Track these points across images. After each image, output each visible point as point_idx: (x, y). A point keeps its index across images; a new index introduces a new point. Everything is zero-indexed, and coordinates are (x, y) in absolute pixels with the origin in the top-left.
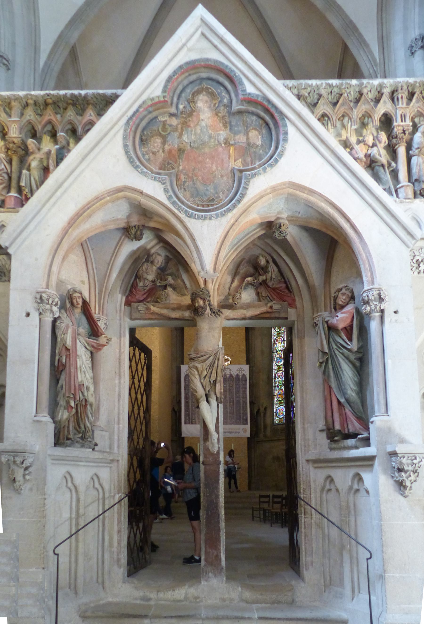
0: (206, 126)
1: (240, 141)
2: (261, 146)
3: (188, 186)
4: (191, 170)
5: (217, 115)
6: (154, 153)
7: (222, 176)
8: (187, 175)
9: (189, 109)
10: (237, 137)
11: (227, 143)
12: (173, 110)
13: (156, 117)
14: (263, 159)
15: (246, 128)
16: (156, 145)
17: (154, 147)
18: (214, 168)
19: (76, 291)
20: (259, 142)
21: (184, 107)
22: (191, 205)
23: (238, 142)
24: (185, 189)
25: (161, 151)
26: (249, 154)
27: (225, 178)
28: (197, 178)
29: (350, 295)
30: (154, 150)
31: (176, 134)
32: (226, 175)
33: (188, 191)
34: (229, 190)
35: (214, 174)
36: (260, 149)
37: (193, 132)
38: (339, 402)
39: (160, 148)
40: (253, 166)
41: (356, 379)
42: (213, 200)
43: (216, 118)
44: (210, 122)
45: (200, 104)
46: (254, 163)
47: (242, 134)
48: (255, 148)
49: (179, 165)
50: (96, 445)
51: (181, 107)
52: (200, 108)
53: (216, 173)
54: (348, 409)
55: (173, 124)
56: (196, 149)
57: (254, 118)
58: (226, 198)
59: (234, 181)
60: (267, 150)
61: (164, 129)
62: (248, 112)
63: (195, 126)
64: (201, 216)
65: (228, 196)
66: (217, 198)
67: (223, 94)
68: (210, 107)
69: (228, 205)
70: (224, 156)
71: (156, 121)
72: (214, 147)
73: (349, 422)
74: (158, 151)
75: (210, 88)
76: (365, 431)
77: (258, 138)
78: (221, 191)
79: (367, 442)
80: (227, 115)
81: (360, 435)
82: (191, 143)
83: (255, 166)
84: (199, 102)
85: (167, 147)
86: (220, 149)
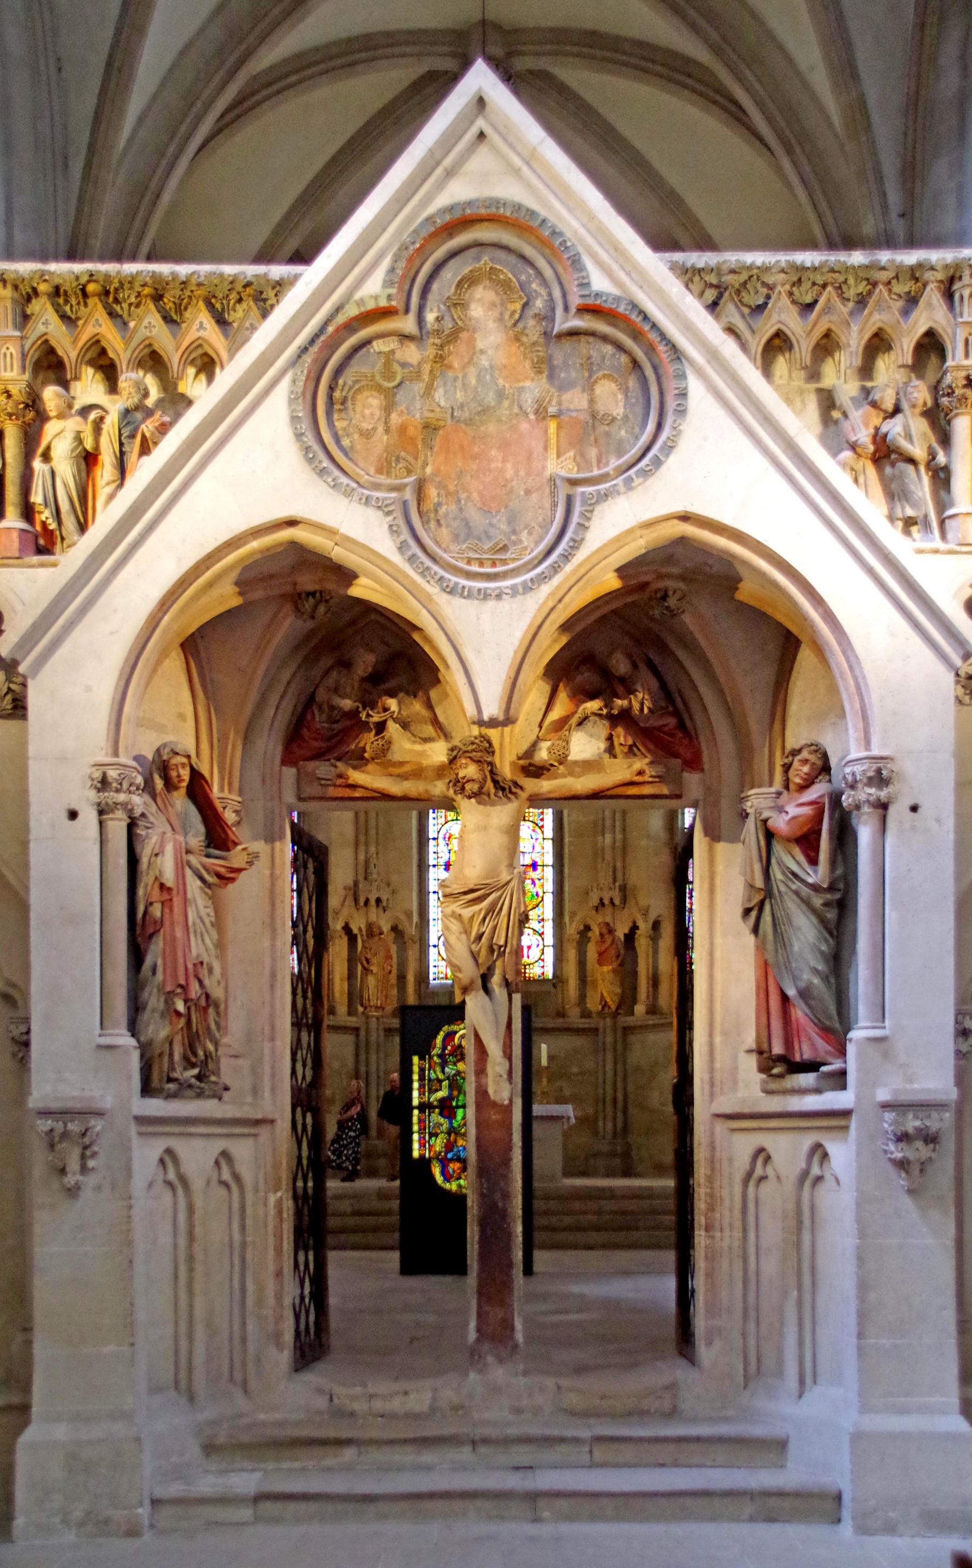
0: (492, 367)
1: (572, 407)
2: (622, 419)
3: (446, 515)
4: (453, 476)
5: (517, 339)
6: (367, 435)
7: (528, 492)
8: (445, 487)
9: (448, 324)
10: (566, 397)
11: (541, 413)
12: (408, 324)
13: (367, 342)
14: (626, 452)
15: (587, 375)
16: (367, 412)
17: (364, 417)
18: (510, 473)
19: (177, 754)
20: (618, 410)
21: (438, 319)
22: (453, 561)
23: (569, 410)
24: (438, 521)
25: (381, 429)
26: (592, 437)
27: (535, 496)
28: (469, 497)
29: (819, 763)
30: (366, 426)
31: (419, 387)
32: (538, 489)
33: (447, 526)
34: (545, 527)
35: (509, 486)
36: (620, 428)
37: (459, 383)
38: (785, 998)
39: (379, 419)
40: (602, 472)
41: (824, 948)
42: (504, 548)
43: (514, 348)
44: (501, 358)
45: (476, 311)
46: (604, 461)
47: (579, 389)
48: (608, 425)
49: (425, 464)
50: (227, 1089)
51: (430, 317)
52: (478, 321)
53: (514, 483)
54: (802, 1010)
55: (410, 360)
56: (466, 424)
57: (609, 349)
58: (537, 543)
59: (554, 505)
60: (637, 430)
61: (388, 373)
62: (593, 334)
63: (464, 368)
64: (475, 592)
65: (541, 539)
66: (515, 543)
67: (534, 286)
68: (501, 319)
69: (540, 563)
70: (533, 443)
71: (368, 352)
72: (510, 420)
73: (803, 1039)
74: (374, 429)
75: (503, 273)
76: (838, 1058)
77: (616, 402)
78: (525, 528)
79: (839, 1080)
80: (542, 340)
81: (825, 1064)
82: (453, 409)
83: (606, 470)
84: (473, 306)
85: (395, 419)
86: (524, 426)
